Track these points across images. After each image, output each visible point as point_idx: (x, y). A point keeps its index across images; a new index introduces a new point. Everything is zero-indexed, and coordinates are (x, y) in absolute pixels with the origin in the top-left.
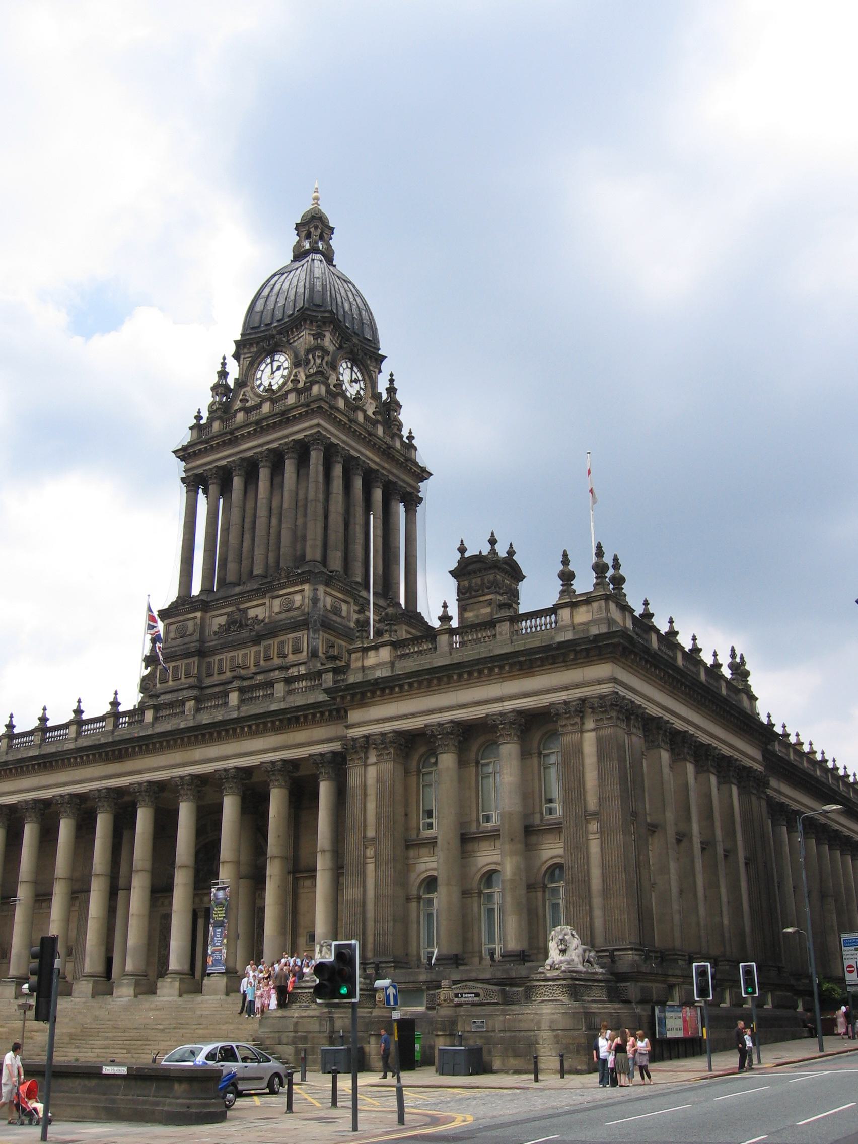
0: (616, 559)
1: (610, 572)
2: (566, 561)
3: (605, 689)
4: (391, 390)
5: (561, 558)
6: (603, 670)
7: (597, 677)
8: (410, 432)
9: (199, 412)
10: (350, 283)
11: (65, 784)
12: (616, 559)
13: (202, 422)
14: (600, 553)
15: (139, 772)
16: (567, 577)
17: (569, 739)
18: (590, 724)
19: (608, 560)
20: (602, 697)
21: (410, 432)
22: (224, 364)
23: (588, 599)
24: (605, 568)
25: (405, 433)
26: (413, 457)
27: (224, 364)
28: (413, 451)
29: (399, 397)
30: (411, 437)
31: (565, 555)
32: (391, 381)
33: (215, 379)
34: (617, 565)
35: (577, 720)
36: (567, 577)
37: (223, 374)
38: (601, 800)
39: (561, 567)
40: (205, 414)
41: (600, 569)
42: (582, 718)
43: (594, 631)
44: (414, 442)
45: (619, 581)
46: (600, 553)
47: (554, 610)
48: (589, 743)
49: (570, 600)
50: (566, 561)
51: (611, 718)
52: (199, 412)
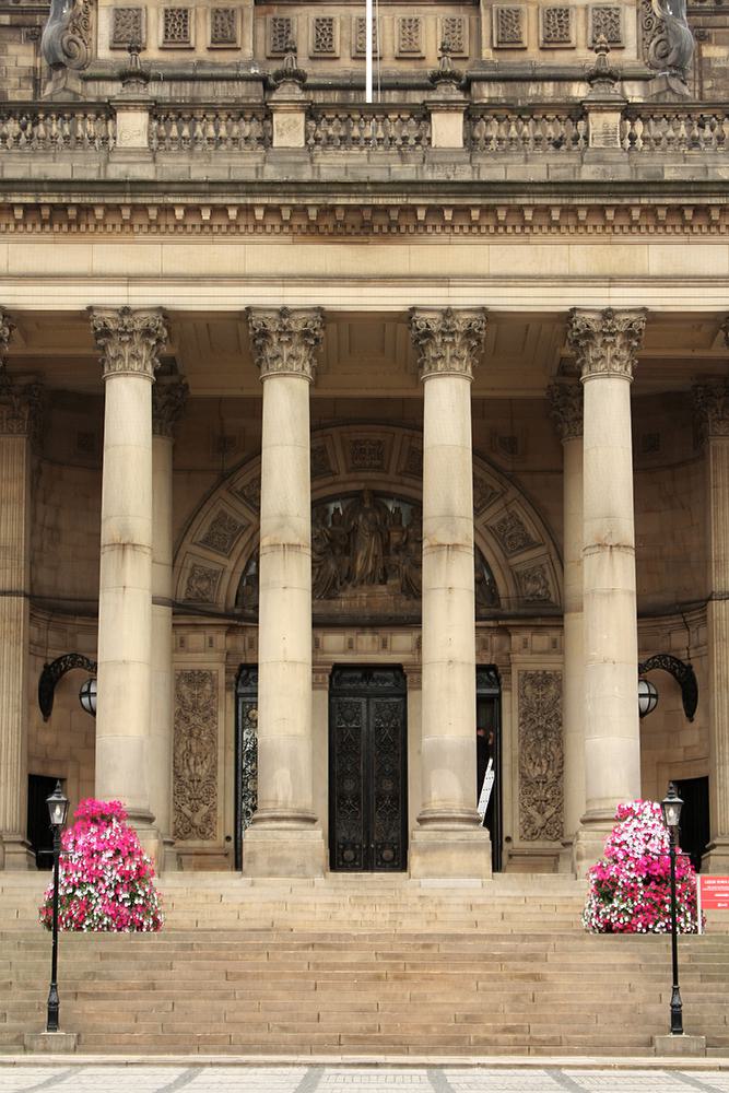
11: (131, 279)
15: (442, 280)
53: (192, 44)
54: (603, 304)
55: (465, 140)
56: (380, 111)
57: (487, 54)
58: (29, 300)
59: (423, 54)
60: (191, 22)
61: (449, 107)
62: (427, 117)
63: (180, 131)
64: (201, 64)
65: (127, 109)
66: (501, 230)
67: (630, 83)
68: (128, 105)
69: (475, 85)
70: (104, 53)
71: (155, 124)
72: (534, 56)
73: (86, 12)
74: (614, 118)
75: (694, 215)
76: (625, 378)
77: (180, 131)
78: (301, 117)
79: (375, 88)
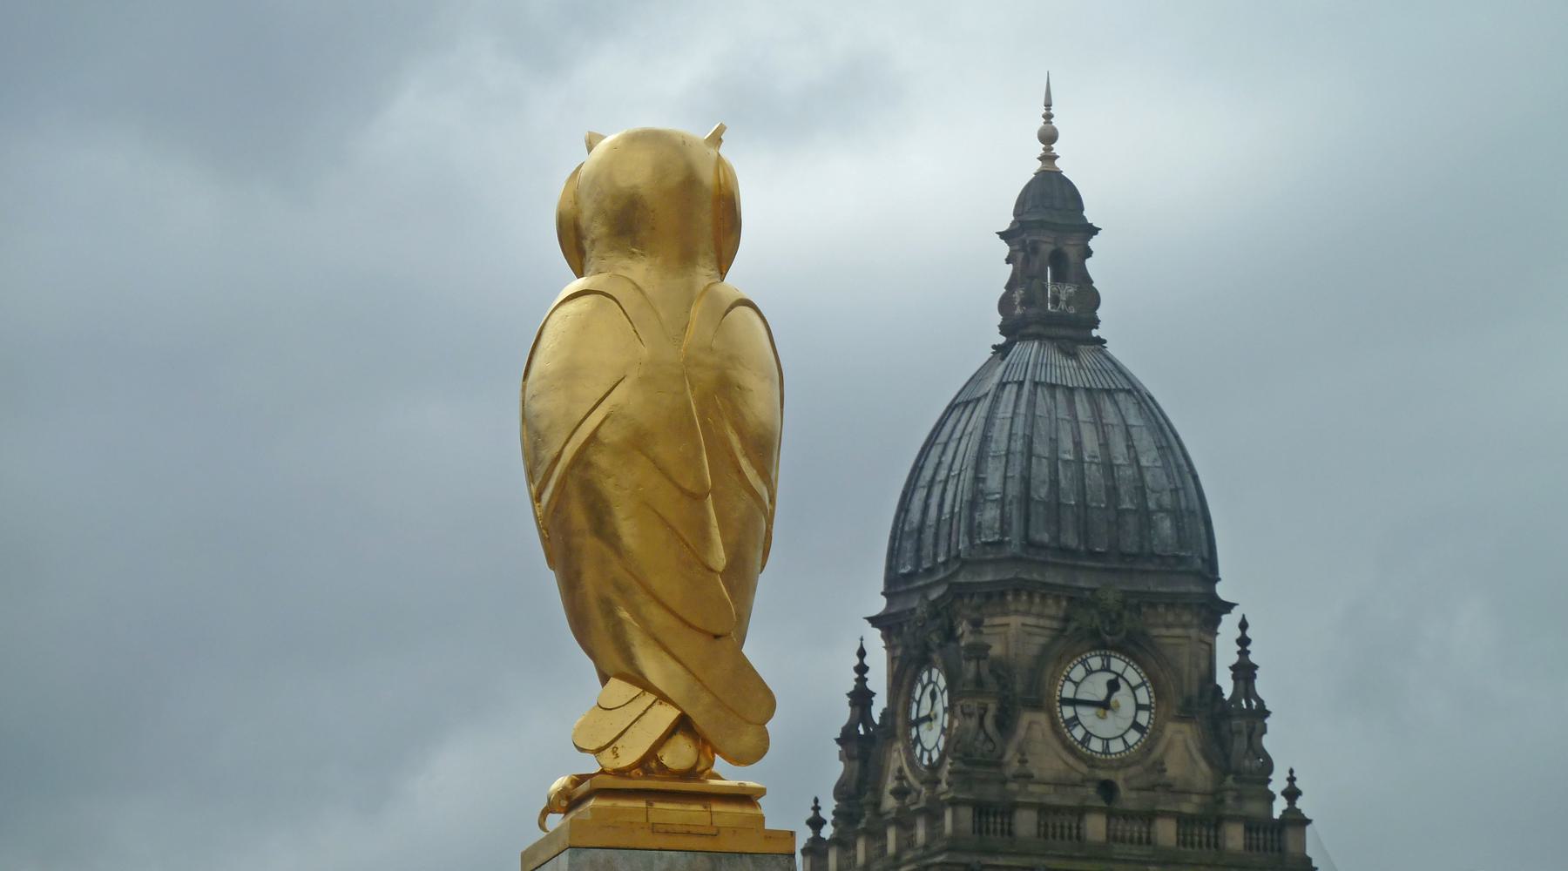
4: (1245, 672)
8: (1292, 779)
9: (816, 809)
10: (1134, 390)
13: (827, 832)
21: (1292, 779)
22: (862, 669)
25: (1277, 784)
26: (1291, 846)
27: (862, 669)
28: (1290, 834)
29: (1261, 686)
30: (1292, 794)
32: (1244, 642)
33: (844, 713)
37: (861, 697)
40: (827, 813)
44: (1299, 804)
52: (816, 809)
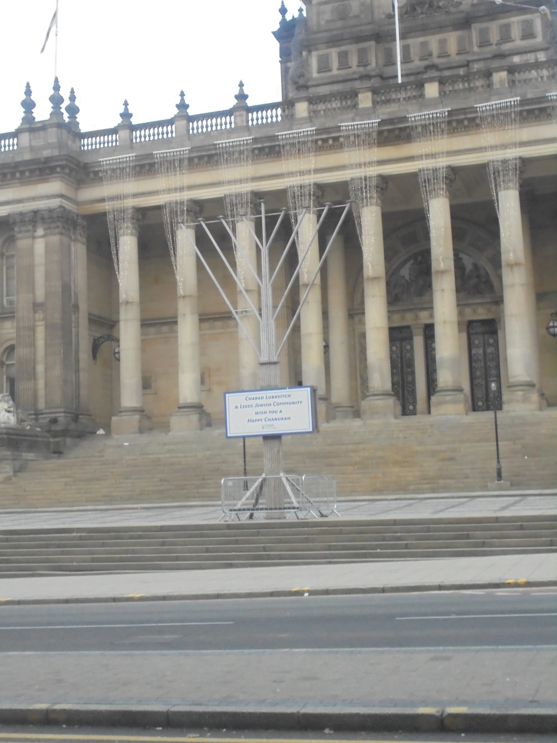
0: (72, 92)
1: (67, 102)
2: (28, 92)
3: (55, 203)
5: (24, 89)
6: (54, 186)
7: (48, 193)
12: (72, 92)
14: (57, 87)
16: (28, 105)
17: (22, 243)
18: (40, 231)
19: (65, 93)
20: (51, 211)
23: (44, 127)
24: (62, 100)
31: (28, 86)
34: (72, 98)
35: (30, 227)
36: (28, 105)
38: (47, 295)
39: (24, 97)
41: (56, 100)
42: (34, 227)
43: (46, 153)
45: (73, 110)
46: (57, 87)
47: (15, 134)
48: (40, 246)
49: (30, 126)
50: (28, 92)
51: (57, 227)
53: (350, 65)
54: (299, 183)
55: (440, 93)
56: (403, 86)
57: (476, 49)
58: (263, 187)
59: (449, 53)
60: (349, 56)
61: (431, 80)
62: (423, 86)
63: (347, 103)
64: (354, 73)
65: (299, 102)
66: (456, 130)
67: (540, 52)
68: (300, 100)
69: (470, 64)
70: (315, 75)
71: (311, 106)
72: (519, 43)
73: (307, 59)
74: (504, 74)
75: (457, 124)
76: (516, 189)
77: (347, 103)
78: (369, 94)
79: (402, 76)
